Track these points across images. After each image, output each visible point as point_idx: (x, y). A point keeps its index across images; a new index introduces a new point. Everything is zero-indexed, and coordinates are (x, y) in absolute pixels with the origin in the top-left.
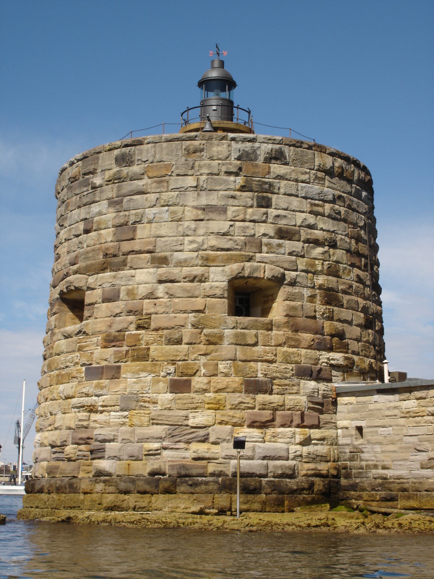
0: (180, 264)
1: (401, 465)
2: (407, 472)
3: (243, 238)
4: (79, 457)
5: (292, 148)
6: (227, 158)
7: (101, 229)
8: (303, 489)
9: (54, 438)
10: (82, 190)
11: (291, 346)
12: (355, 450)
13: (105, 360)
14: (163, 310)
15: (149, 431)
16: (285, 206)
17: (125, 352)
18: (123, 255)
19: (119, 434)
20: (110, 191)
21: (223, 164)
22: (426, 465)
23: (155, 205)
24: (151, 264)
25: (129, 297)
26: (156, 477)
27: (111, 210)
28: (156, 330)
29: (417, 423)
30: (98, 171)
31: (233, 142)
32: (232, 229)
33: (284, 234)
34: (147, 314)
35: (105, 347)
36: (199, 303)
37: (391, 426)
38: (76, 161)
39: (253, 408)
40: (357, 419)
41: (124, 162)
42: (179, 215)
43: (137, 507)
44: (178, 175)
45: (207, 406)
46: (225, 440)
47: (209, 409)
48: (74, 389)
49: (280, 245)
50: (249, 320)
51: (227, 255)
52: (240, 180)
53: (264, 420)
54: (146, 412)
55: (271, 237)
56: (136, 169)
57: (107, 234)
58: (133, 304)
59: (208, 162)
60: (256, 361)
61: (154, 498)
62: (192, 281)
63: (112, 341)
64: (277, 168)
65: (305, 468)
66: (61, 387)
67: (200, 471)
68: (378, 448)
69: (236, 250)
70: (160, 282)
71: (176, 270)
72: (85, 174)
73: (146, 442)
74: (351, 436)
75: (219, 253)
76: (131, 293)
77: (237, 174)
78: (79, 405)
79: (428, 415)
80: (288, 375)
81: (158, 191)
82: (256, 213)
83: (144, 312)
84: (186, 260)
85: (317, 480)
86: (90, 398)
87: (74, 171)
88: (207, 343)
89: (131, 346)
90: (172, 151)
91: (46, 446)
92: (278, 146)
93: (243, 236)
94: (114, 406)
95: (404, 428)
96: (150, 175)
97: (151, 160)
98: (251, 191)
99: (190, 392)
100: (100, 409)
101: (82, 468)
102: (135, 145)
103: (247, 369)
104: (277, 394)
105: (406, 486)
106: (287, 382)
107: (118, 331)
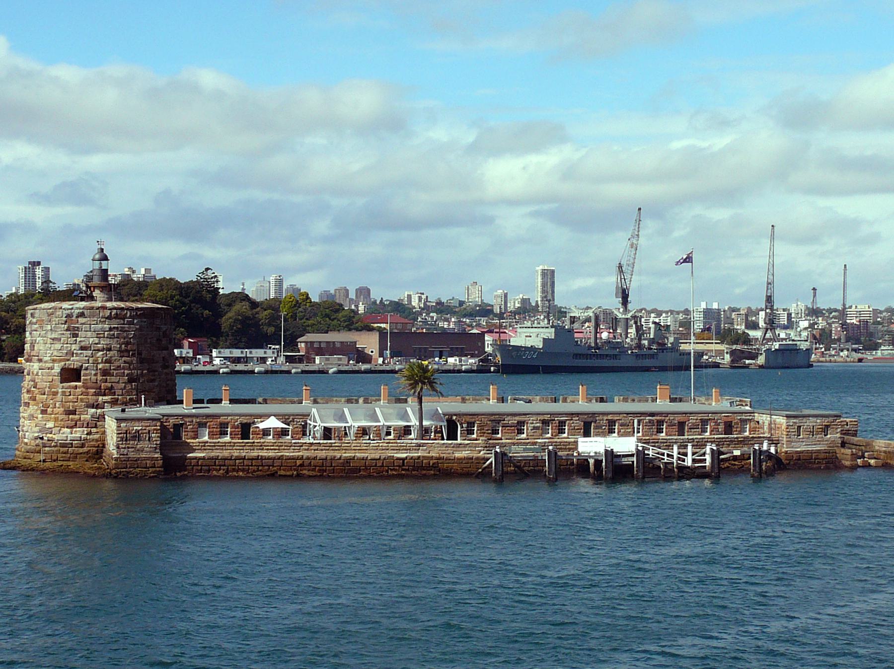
0: (46, 362)
33: (83, 348)
64: (81, 320)
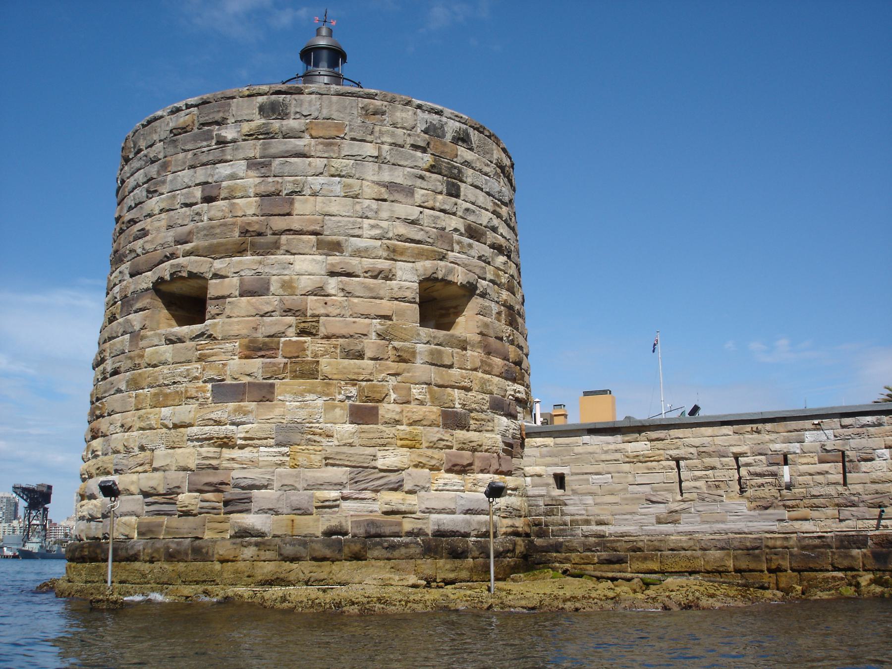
0: (358, 253)
1: (627, 519)
2: (637, 528)
3: (435, 230)
4: (203, 510)
5: (476, 132)
6: (413, 128)
7: (234, 198)
8: (508, 551)
9: (153, 483)
10: (199, 145)
11: (485, 372)
12: (554, 503)
13: (249, 375)
14: (338, 311)
15: (324, 475)
16: (473, 200)
17: (282, 365)
18: (274, 234)
19: (275, 478)
21: (409, 135)
22: (666, 519)
23: (322, 173)
24: (318, 249)
25: (284, 290)
26: (334, 537)
27: (250, 173)
28: (328, 337)
29: (649, 469)
30: (229, 121)
31: (419, 110)
32: (421, 216)
33: (474, 233)
34: (313, 316)
35: (247, 357)
36: (386, 307)
37: (609, 473)
38: (184, 108)
39: (451, 447)
40: (556, 465)
41: (274, 113)
42: (356, 190)
43: (312, 579)
44: (353, 139)
45: (400, 443)
46: (424, 488)
47: (402, 446)
48: (192, 415)
49: (470, 246)
50: (445, 335)
51: (417, 247)
52: (426, 159)
53: (465, 463)
54: (316, 448)
55: (461, 234)
56: (292, 123)
57: (248, 206)
58: (291, 301)
59: (391, 129)
60: (453, 387)
61: (336, 567)
62: (375, 277)
63: (260, 349)
64: (463, 153)
65: (504, 524)
66: (165, 411)
67: (396, 529)
68: (589, 500)
69: (427, 243)
70: (332, 274)
71: (355, 261)
72: (203, 124)
73: (319, 489)
74: (548, 485)
75: (407, 244)
76: (288, 286)
77: (424, 150)
78: (204, 436)
79: (668, 460)
80: (485, 408)
81: (326, 155)
82: (448, 202)
83: (309, 313)
84: (366, 249)
85: (518, 540)
86: (224, 427)
87: (182, 120)
88: (398, 359)
89: (290, 358)
90: (345, 108)
91: (132, 494)
92: (464, 127)
93: (434, 228)
94: (266, 439)
95: (630, 475)
96: (314, 134)
97: (315, 114)
98: (440, 174)
99: (377, 424)
100: (239, 442)
101: (207, 524)
102: (291, 94)
103: (445, 397)
104: (475, 431)
105: (641, 544)
106: (483, 416)
107: (268, 337)
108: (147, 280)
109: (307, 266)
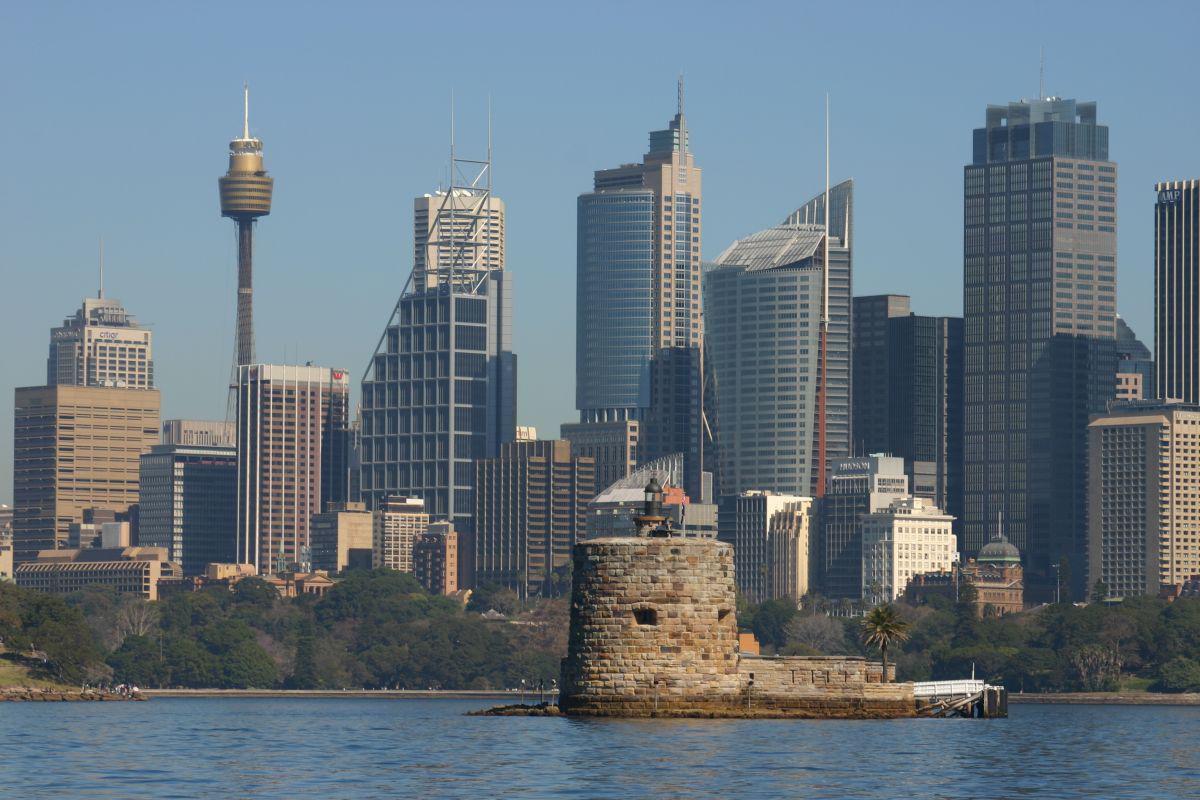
20: (670, 566)
56: (682, 557)
57: (669, 586)
66: (645, 655)
70: (696, 610)
76: (683, 615)
108: (629, 607)
109: (688, 608)
